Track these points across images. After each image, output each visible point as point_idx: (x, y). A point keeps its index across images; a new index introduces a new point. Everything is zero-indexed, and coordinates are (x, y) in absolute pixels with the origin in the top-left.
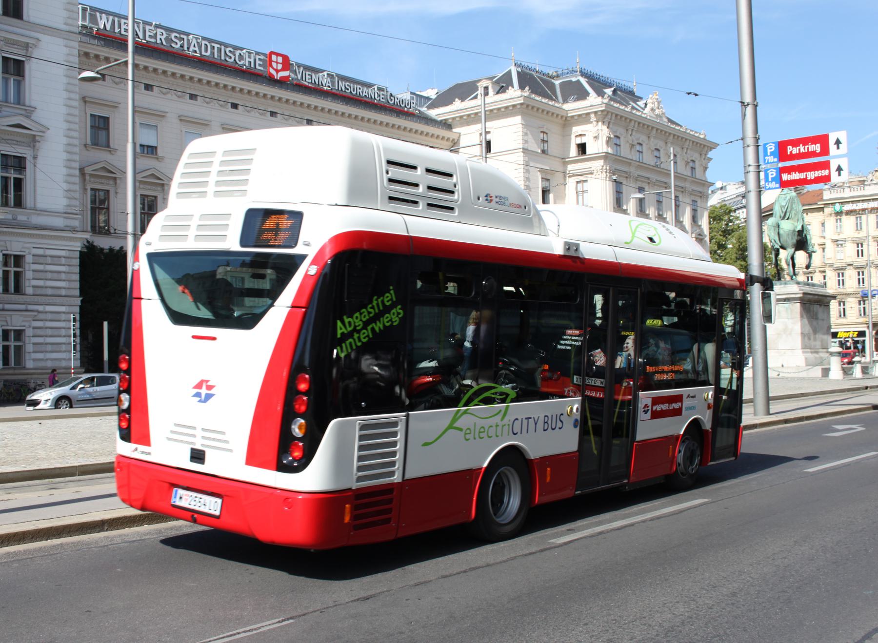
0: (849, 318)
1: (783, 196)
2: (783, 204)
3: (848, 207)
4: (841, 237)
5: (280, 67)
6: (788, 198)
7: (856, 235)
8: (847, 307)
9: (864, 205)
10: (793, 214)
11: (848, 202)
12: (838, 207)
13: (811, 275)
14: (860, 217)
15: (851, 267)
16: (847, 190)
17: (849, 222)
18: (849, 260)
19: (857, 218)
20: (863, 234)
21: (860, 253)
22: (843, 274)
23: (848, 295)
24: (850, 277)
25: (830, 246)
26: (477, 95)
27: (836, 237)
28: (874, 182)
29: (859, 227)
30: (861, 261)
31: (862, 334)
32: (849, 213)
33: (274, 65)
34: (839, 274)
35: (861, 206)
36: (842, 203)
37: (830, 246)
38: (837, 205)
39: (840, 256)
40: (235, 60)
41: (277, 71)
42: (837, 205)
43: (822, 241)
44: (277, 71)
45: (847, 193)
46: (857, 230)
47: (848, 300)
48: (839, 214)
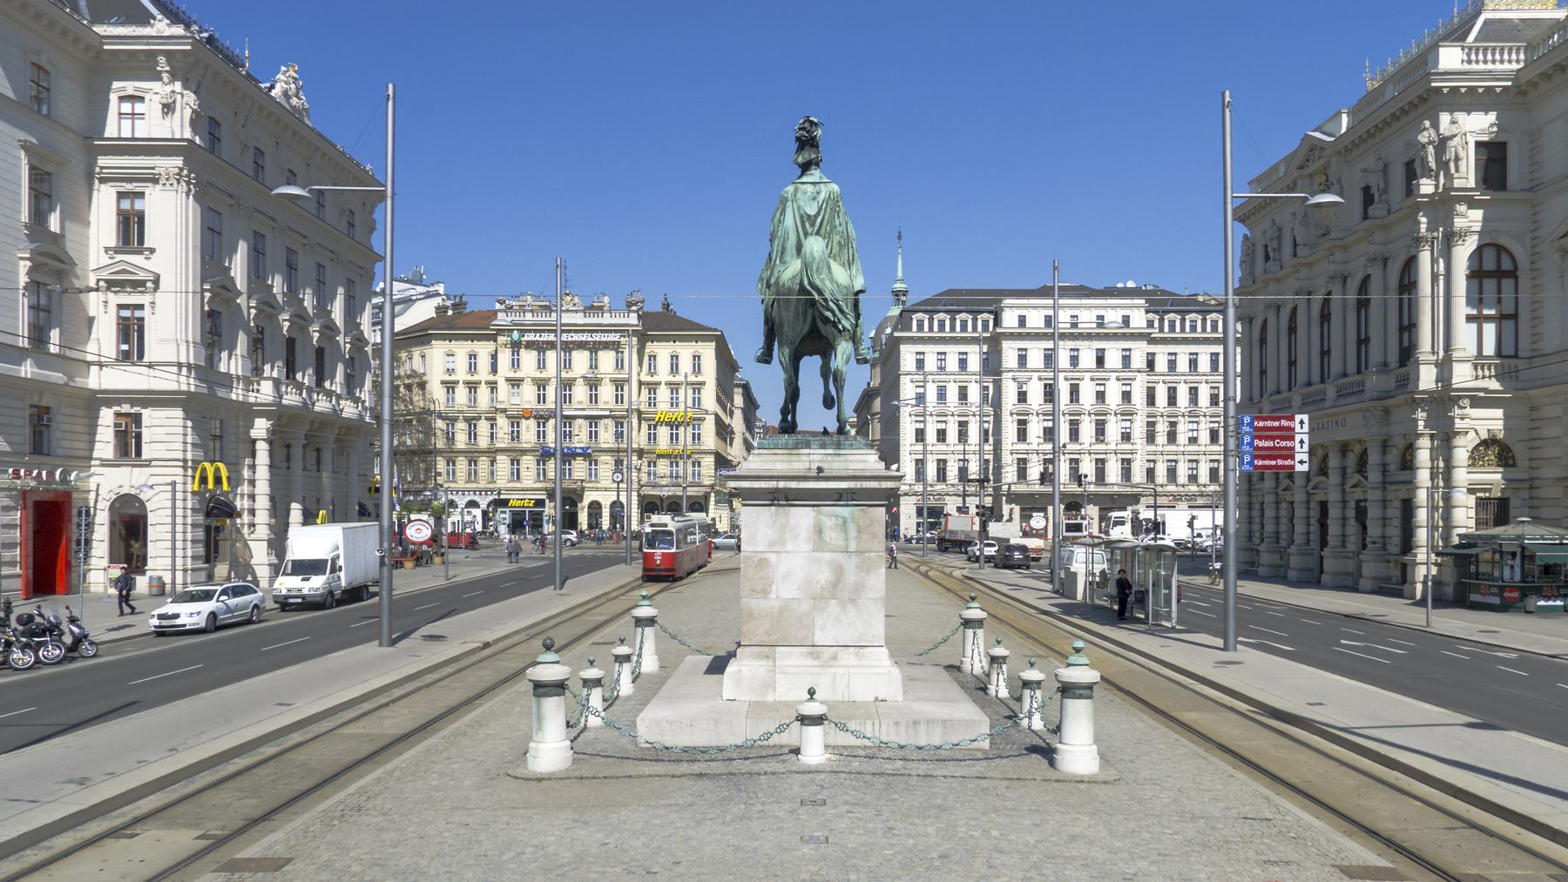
0: (524, 482)
1: (810, 188)
2: (812, 211)
4: (519, 375)
6: (822, 196)
7: (538, 375)
8: (523, 467)
10: (835, 243)
11: (530, 331)
13: (474, 422)
21: (541, 398)
23: (524, 452)
24: (528, 428)
25: (503, 387)
27: (512, 375)
29: (541, 365)
31: (540, 503)
32: (530, 345)
34: (513, 424)
36: (521, 330)
37: (503, 387)
38: (515, 332)
39: (516, 400)
42: (515, 332)
43: (491, 378)
46: (539, 368)
47: (524, 457)
48: (516, 346)
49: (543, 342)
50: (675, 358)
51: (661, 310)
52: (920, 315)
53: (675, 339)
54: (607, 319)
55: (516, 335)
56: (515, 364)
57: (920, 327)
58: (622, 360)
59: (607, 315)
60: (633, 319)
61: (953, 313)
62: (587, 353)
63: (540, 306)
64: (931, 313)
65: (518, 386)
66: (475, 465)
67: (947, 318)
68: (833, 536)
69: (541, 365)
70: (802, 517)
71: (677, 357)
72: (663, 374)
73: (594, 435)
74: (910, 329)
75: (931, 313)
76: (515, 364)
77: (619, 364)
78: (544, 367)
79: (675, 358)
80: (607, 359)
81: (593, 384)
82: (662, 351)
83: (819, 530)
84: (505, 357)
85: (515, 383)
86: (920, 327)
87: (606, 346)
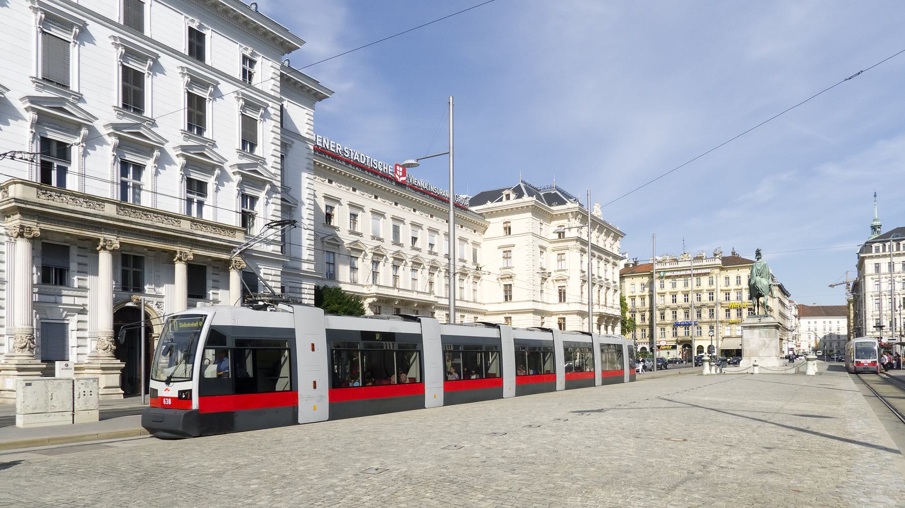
3: (668, 274)
4: (663, 291)
5: (401, 174)
9: (678, 273)
12: (662, 274)
14: (700, 278)
15: (669, 309)
16: (668, 264)
17: (668, 283)
18: (668, 305)
19: (697, 278)
20: (689, 288)
21: (674, 301)
22: (676, 312)
26: (502, 198)
28: (683, 260)
29: (674, 286)
30: (674, 305)
33: (398, 172)
35: (676, 273)
38: (662, 272)
40: (378, 168)
41: (400, 177)
42: (662, 272)
44: (400, 177)
45: (668, 266)
49: (675, 276)
50: (739, 277)
51: (731, 255)
52: (877, 244)
53: (738, 269)
54: (705, 263)
55: (662, 274)
56: (662, 286)
57: (877, 250)
58: (712, 281)
59: (704, 261)
60: (718, 262)
61: (898, 242)
62: (695, 279)
63: (672, 259)
64: (884, 242)
65: (663, 296)
66: (645, 332)
67: (894, 244)
68: (763, 334)
69: (674, 286)
70: (756, 331)
71: (740, 277)
72: (733, 285)
73: (699, 315)
74: (871, 252)
75: (884, 242)
76: (662, 286)
77: (711, 283)
78: (675, 287)
79: (739, 277)
80: (705, 280)
81: (698, 293)
82: (732, 274)
83: (760, 334)
84: (657, 283)
85: (662, 295)
86: (877, 250)
87: (705, 274)
